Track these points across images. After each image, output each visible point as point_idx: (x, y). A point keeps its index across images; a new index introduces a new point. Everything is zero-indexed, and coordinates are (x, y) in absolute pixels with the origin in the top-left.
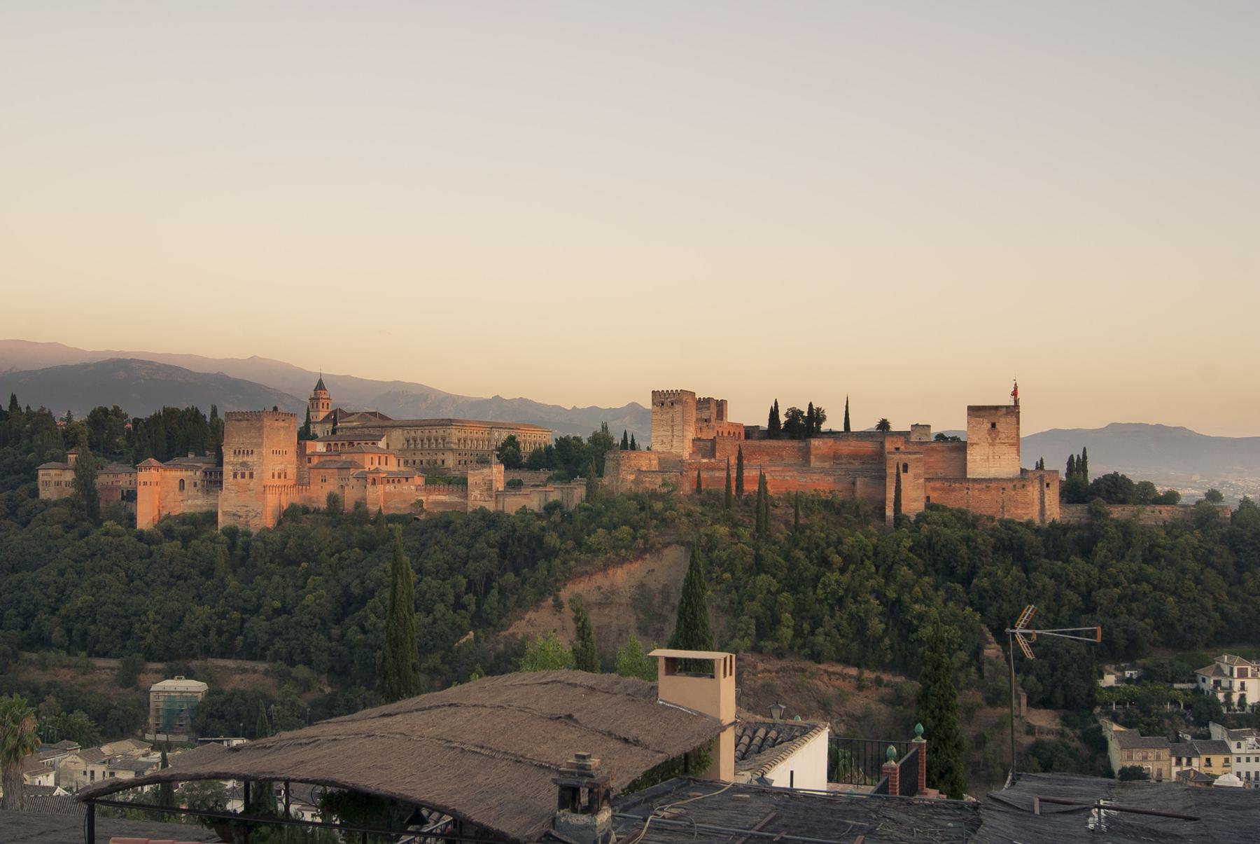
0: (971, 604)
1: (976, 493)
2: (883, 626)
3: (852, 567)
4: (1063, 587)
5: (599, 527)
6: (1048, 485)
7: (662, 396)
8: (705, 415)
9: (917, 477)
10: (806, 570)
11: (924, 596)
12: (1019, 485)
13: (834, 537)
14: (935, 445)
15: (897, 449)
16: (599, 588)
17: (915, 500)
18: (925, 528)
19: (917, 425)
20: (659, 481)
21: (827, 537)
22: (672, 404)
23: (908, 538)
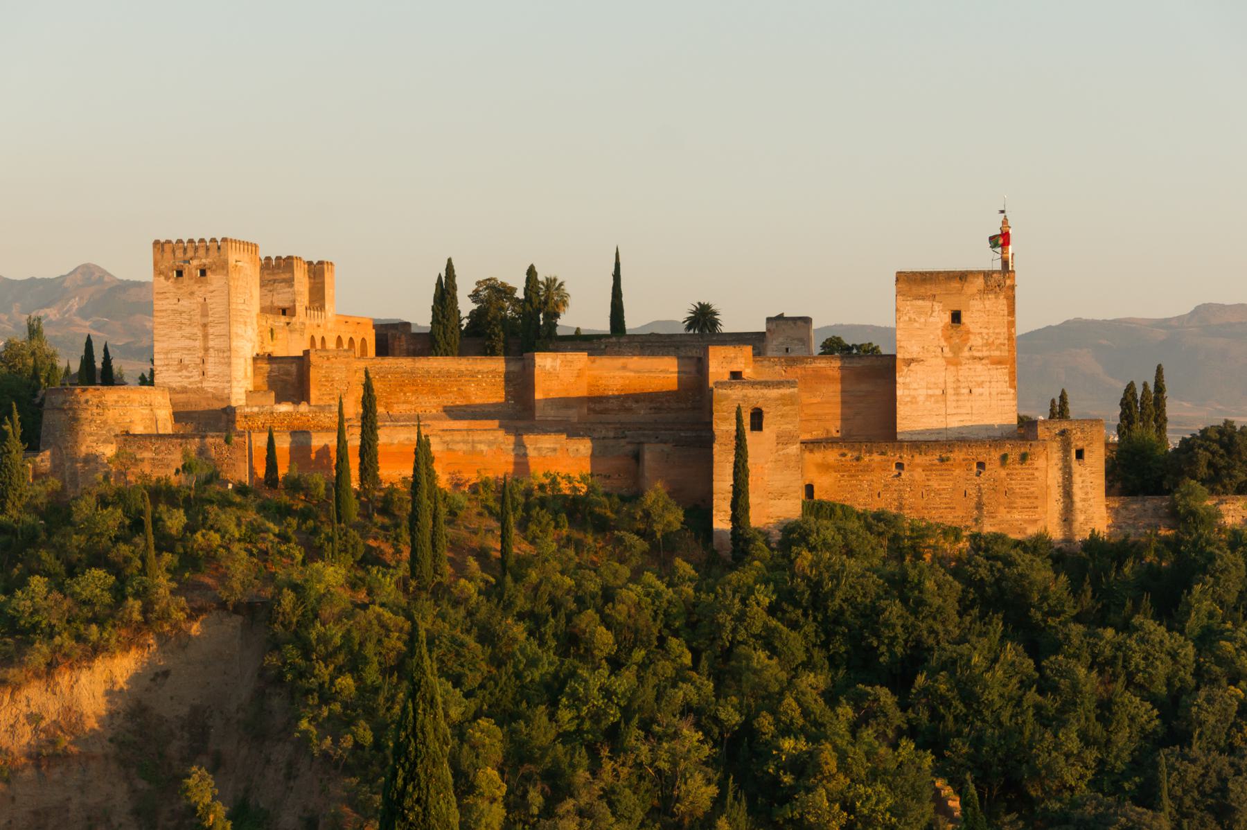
0: (912, 731)
1: (919, 475)
2: (713, 790)
3: (639, 655)
4: (1119, 686)
5: (32, 572)
6: (1080, 454)
7: (179, 254)
8: (281, 300)
9: (783, 439)
10: (533, 663)
11: (806, 713)
12: (1014, 455)
13: (593, 585)
14: (822, 364)
15: (736, 375)
16: (34, 719)
17: (781, 495)
18: (805, 559)
19: (780, 317)
20: (176, 459)
21: (579, 585)
22: (203, 273)
23: (766, 583)
